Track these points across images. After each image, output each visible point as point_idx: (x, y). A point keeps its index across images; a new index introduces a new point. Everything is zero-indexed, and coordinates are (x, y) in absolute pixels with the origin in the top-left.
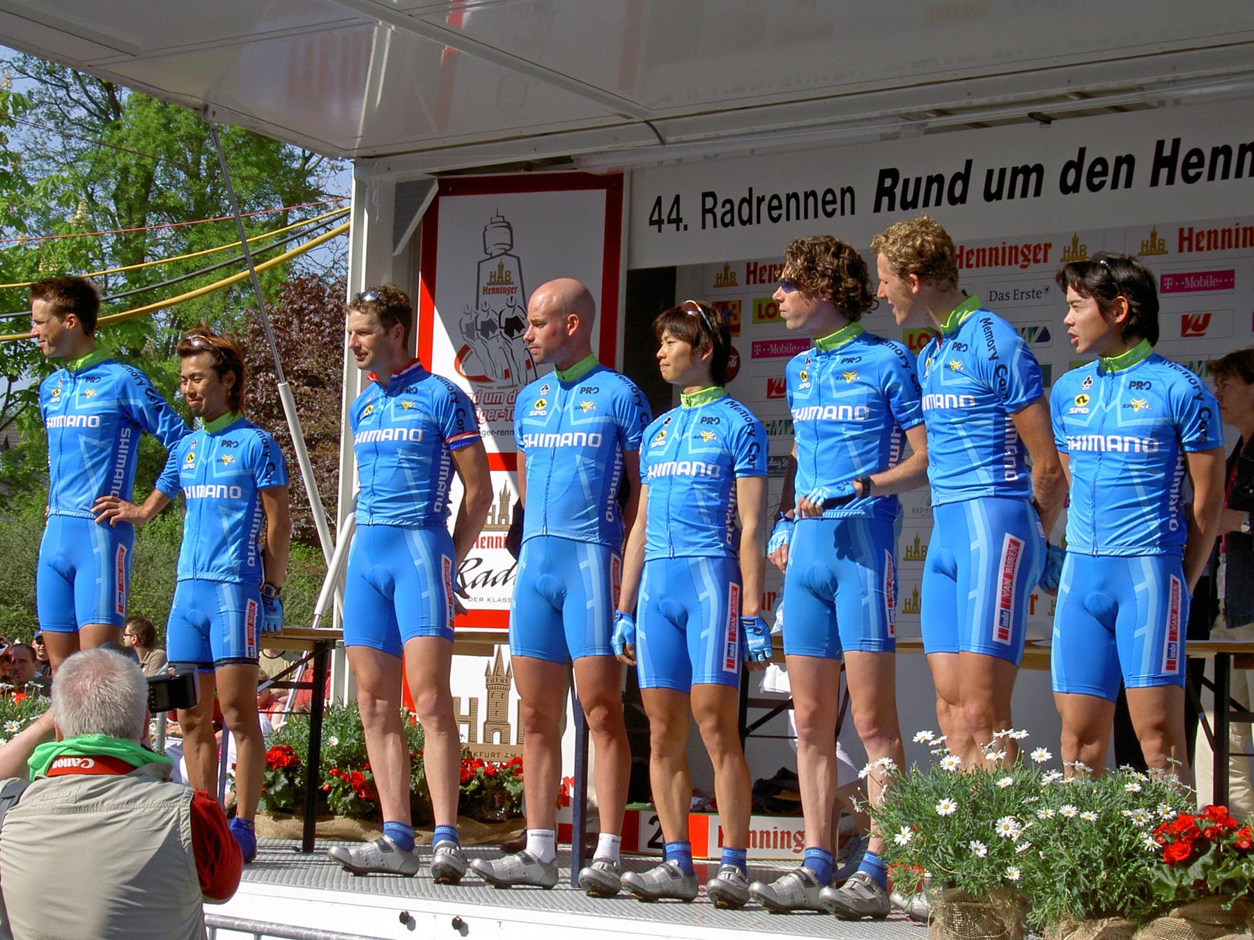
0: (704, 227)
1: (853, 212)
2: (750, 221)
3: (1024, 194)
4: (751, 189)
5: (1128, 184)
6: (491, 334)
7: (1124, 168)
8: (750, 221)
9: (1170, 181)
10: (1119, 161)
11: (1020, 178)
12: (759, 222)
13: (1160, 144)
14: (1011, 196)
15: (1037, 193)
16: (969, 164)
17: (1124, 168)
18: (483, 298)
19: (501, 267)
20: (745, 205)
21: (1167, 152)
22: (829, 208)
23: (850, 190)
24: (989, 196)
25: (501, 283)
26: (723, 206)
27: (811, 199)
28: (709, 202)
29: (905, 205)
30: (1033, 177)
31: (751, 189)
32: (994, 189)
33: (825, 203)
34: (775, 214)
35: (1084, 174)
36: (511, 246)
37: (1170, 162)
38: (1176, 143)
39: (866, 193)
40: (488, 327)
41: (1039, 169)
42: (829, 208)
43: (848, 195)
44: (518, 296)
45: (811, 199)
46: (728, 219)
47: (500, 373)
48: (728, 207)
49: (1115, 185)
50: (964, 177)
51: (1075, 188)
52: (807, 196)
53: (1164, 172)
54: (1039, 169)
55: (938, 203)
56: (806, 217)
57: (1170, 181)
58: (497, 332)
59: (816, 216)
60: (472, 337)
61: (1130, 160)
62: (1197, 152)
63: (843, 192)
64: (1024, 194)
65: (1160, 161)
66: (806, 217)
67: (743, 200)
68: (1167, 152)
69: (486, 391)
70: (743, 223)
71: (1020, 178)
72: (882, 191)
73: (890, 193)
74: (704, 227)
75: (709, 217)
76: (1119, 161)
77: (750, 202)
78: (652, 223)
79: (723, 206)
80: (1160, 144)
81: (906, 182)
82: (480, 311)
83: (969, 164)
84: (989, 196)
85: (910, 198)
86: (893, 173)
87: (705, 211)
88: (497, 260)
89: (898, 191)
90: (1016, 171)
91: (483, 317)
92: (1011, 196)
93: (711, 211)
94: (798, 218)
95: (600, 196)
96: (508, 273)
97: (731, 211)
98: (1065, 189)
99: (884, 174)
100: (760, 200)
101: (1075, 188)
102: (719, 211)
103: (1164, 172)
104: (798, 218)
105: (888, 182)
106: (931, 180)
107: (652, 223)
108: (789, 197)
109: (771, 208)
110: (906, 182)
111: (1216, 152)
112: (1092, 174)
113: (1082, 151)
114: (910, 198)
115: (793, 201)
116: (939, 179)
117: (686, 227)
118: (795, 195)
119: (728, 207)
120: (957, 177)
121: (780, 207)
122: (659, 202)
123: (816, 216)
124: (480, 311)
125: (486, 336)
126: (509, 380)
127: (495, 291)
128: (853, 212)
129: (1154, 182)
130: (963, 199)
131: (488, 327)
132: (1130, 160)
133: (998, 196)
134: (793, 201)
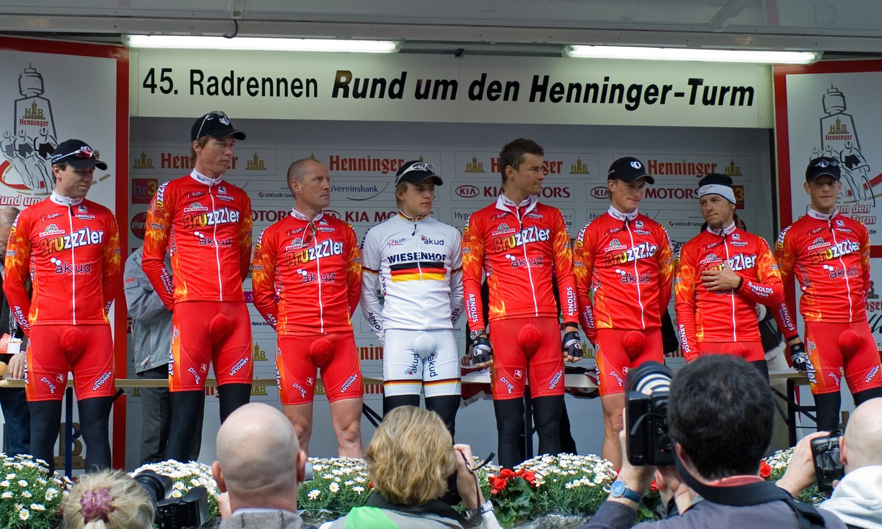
0: (192, 93)
1: (316, 95)
2: (232, 93)
3: (444, 97)
4: (232, 72)
5: (515, 98)
6: (28, 155)
7: (512, 89)
8: (232, 93)
9: (543, 99)
10: (509, 85)
11: (441, 87)
12: (239, 94)
13: (536, 78)
14: (435, 97)
15: (453, 97)
16: (404, 75)
17: (512, 89)
18: (20, 127)
19: (34, 105)
20: (228, 83)
21: (540, 82)
22: (297, 91)
23: (314, 81)
24: (418, 96)
25: (33, 117)
26: (209, 80)
27: (282, 84)
28: (197, 77)
29: (356, 95)
30: (450, 88)
31: (232, 72)
32: (422, 92)
33: (293, 87)
34: (253, 90)
35: (481, 89)
36: (43, 91)
37: (543, 89)
38: (546, 78)
39: (326, 85)
40: (24, 150)
41: (454, 84)
42: (297, 91)
43: (312, 85)
44: (49, 127)
45: (282, 84)
46: (213, 89)
47: (36, 183)
48: (213, 82)
49: (506, 98)
50: (401, 82)
51: (479, 97)
52: (279, 81)
53: (538, 95)
54: (454, 84)
55: (382, 95)
56: (278, 95)
57: (543, 99)
58: (33, 153)
59: (286, 95)
60: (12, 155)
61: (516, 85)
62: (559, 85)
63: (308, 82)
64: (444, 97)
65: (535, 88)
66: (278, 95)
67: (226, 79)
68: (540, 82)
69: (24, 196)
70: (226, 94)
71: (441, 87)
72: (338, 85)
73: (345, 87)
74: (192, 93)
75: (197, 88)
76: (509, 85)
77: (232, 81)
78: (145, 86)
79: (209, 80)
80: (536, 78)
81: (357, 81)
82: (17, 137)
83: (404, 75)
84: (418, 96)
85: (360, 90)
86: (348, 74)
87: (193, 83)
88: (32, 100)
89: (351, 86)
90: (438, 83)
91: (20, 142)
92: (435, 97)
93: (199, 83)
94: (272, 94)
95: (110, 65)
96: (41, 111)
97: (216, 84)
98: (472, 97)
99: (340, 73)
100: (240, 80)
101: (479, 97)
102: (205, 84)
103: (538, 95)
104: (272, 94)
105: (343, 79)
106: (376, 82)
107: (145, 86)
108: (264, 81)
109: (249, 86)
110: (357, 81)
111: (571, 86)
112: (490, 90)
113: (484, 76)
114: (360, 90)
115: (268, 84)
116: (383, 82)
117: (176, 92)
118: (269, 80)
119: (213, 82)
120: (395, 82)
121: (257, 86)
122: (152, 72)
123: (286, 95)
124: (17, 137)
125: (24, 155)
126: (45, 189)
127: (32, 123)
128: (316, 95)
129: (532, 99)
130: (400, 95)
131: (24, 150)
132: (516, 85)
133: (425, 96)
134: (268, 84)
